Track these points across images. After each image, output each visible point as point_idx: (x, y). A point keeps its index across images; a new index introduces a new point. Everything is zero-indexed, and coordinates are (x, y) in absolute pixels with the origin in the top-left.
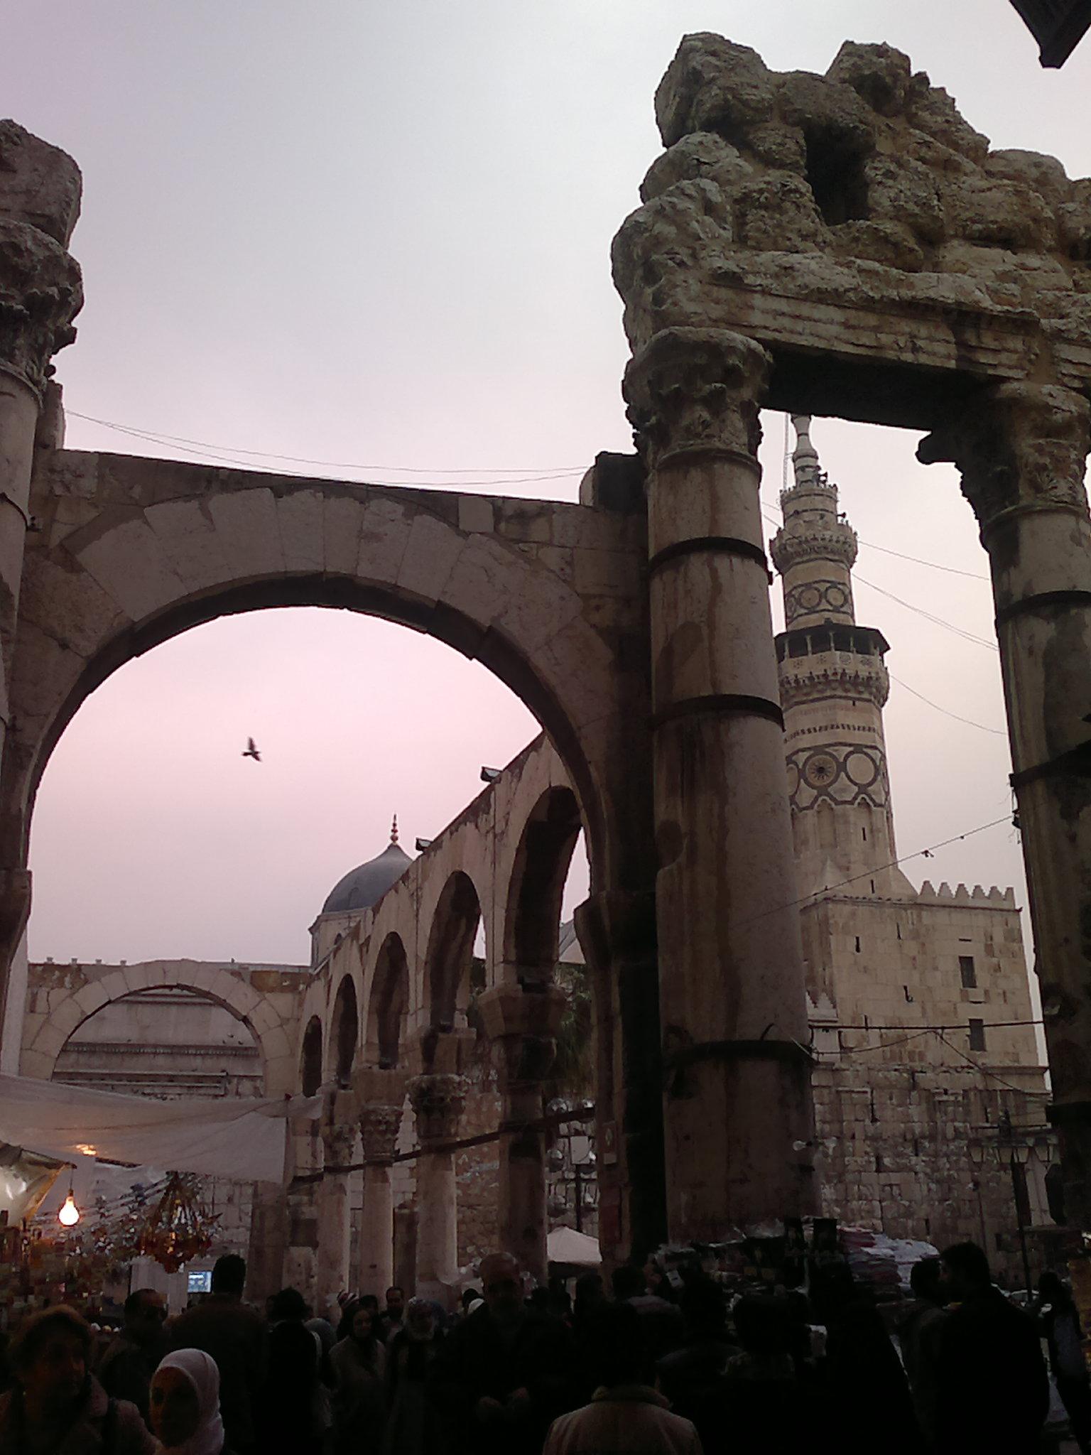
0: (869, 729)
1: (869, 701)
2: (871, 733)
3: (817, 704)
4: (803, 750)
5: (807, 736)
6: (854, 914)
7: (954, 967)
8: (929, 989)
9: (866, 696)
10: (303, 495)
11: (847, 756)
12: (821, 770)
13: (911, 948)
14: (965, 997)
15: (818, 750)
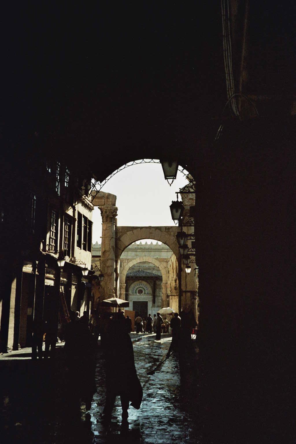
10: (144, 229)
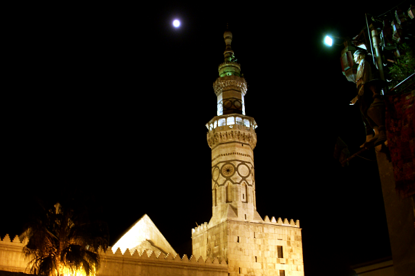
1: (248, 145)
3: (228, 145)
5: (223, 157)
6: (237, 228)
7: (275, 250)
8: (266, 258)
9: (247, 142)
12: (228, 170)
13: (259, 241)
14: (278, 262)
15: (228, 162)
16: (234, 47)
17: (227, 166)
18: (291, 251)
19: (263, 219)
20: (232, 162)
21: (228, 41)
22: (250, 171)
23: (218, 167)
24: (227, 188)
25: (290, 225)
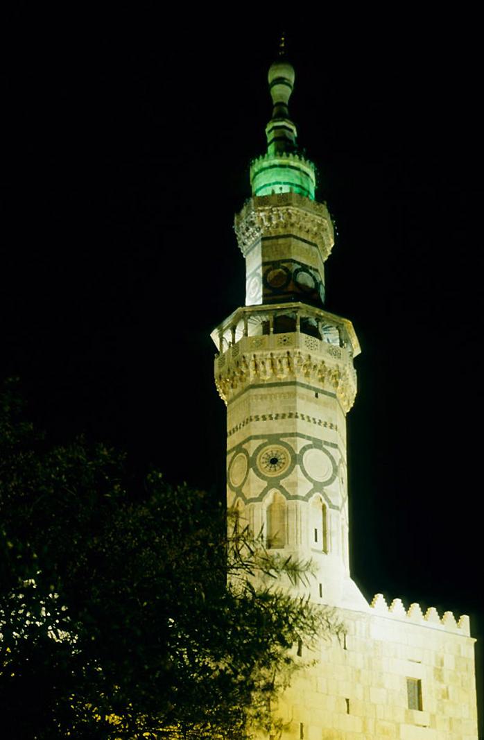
0: (331, 426)
2: (333, 431)
3: (274, 390)
4: (257, 437)
9: (331, 389)
11: (304, 449)
12: (274, 461)
14: (410, 720)
15: (274, 439)
16: (295, 109)
17: (272, 449)
18: (446, 695)
19: (370, 598)
20: (285, 440)
21: (282, 93)
22: (336, 470)
23: (246, 452)
24: (270, 509)
25: (442, 627)
